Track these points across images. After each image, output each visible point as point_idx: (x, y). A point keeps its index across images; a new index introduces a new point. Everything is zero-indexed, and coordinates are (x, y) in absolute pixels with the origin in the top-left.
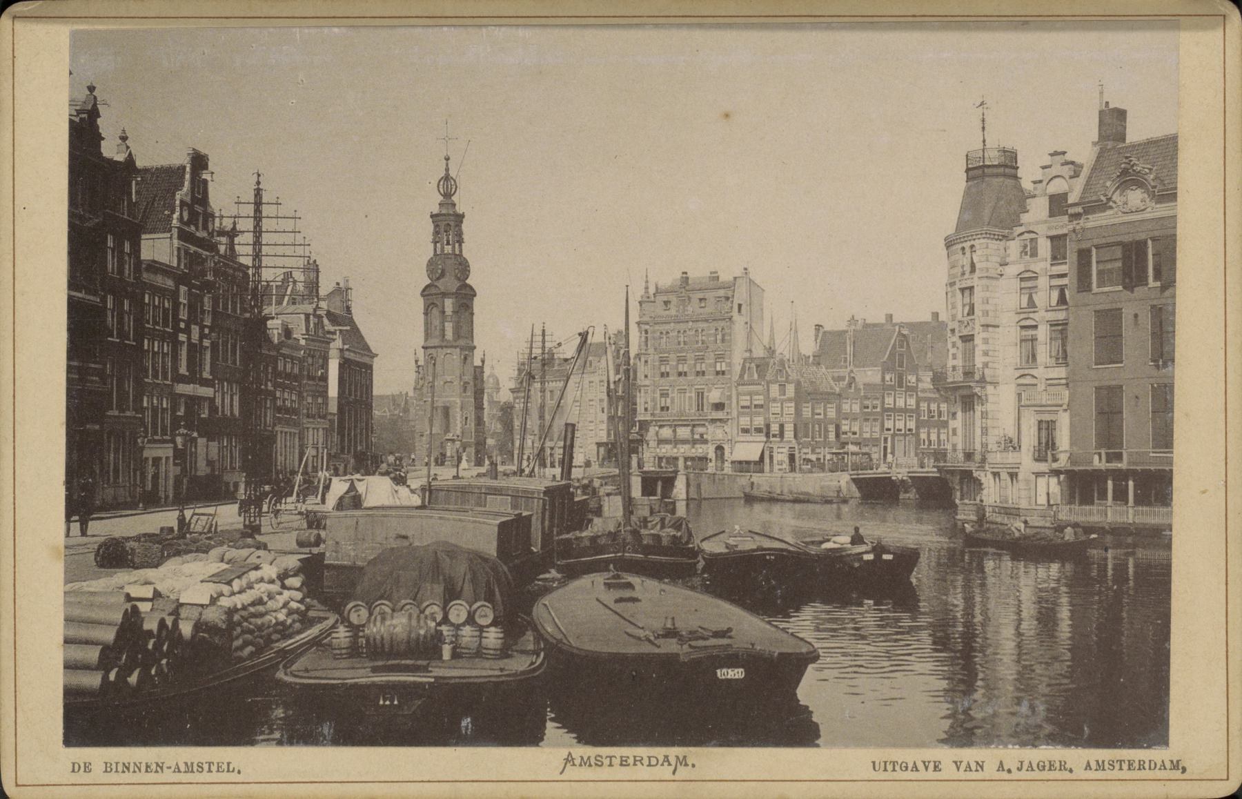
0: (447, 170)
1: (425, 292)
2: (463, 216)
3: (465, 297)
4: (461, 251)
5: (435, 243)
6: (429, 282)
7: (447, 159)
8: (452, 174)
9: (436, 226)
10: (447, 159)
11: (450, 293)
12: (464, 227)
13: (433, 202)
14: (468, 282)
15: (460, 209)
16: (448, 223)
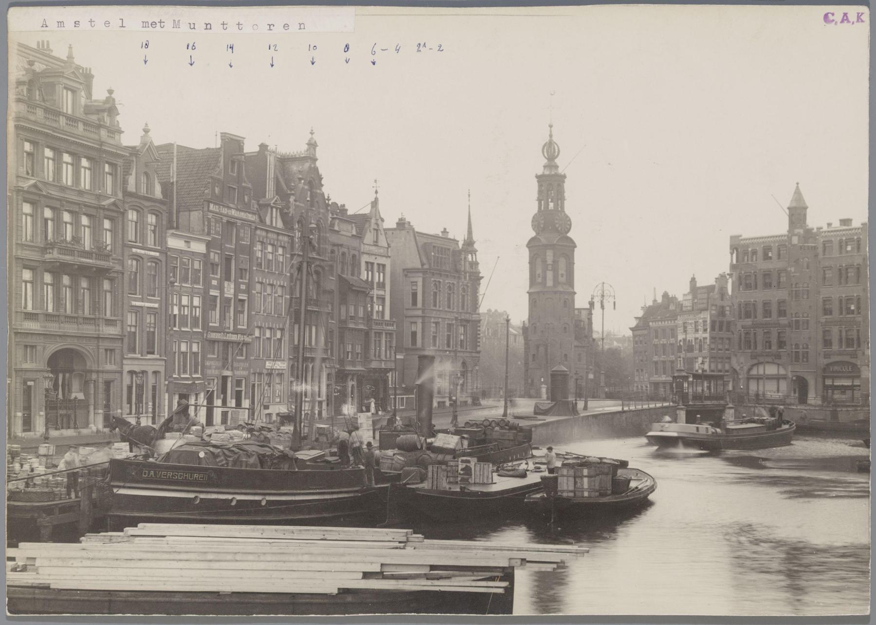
0: (551, 136)
1: (532, 244)
2: (564, 177)
3: (567, 249)
4: (562, 207)
5: (539, 200)
6: (533, 234)
7: (551, 126)
8: (554, 139)
9: (540, 186)
10: (551, 126)
11: (552, 245)
12: (567, 185)
13: (539, 165)
14: (569, 235)
15: (560, 171)
16: (551, 185)
